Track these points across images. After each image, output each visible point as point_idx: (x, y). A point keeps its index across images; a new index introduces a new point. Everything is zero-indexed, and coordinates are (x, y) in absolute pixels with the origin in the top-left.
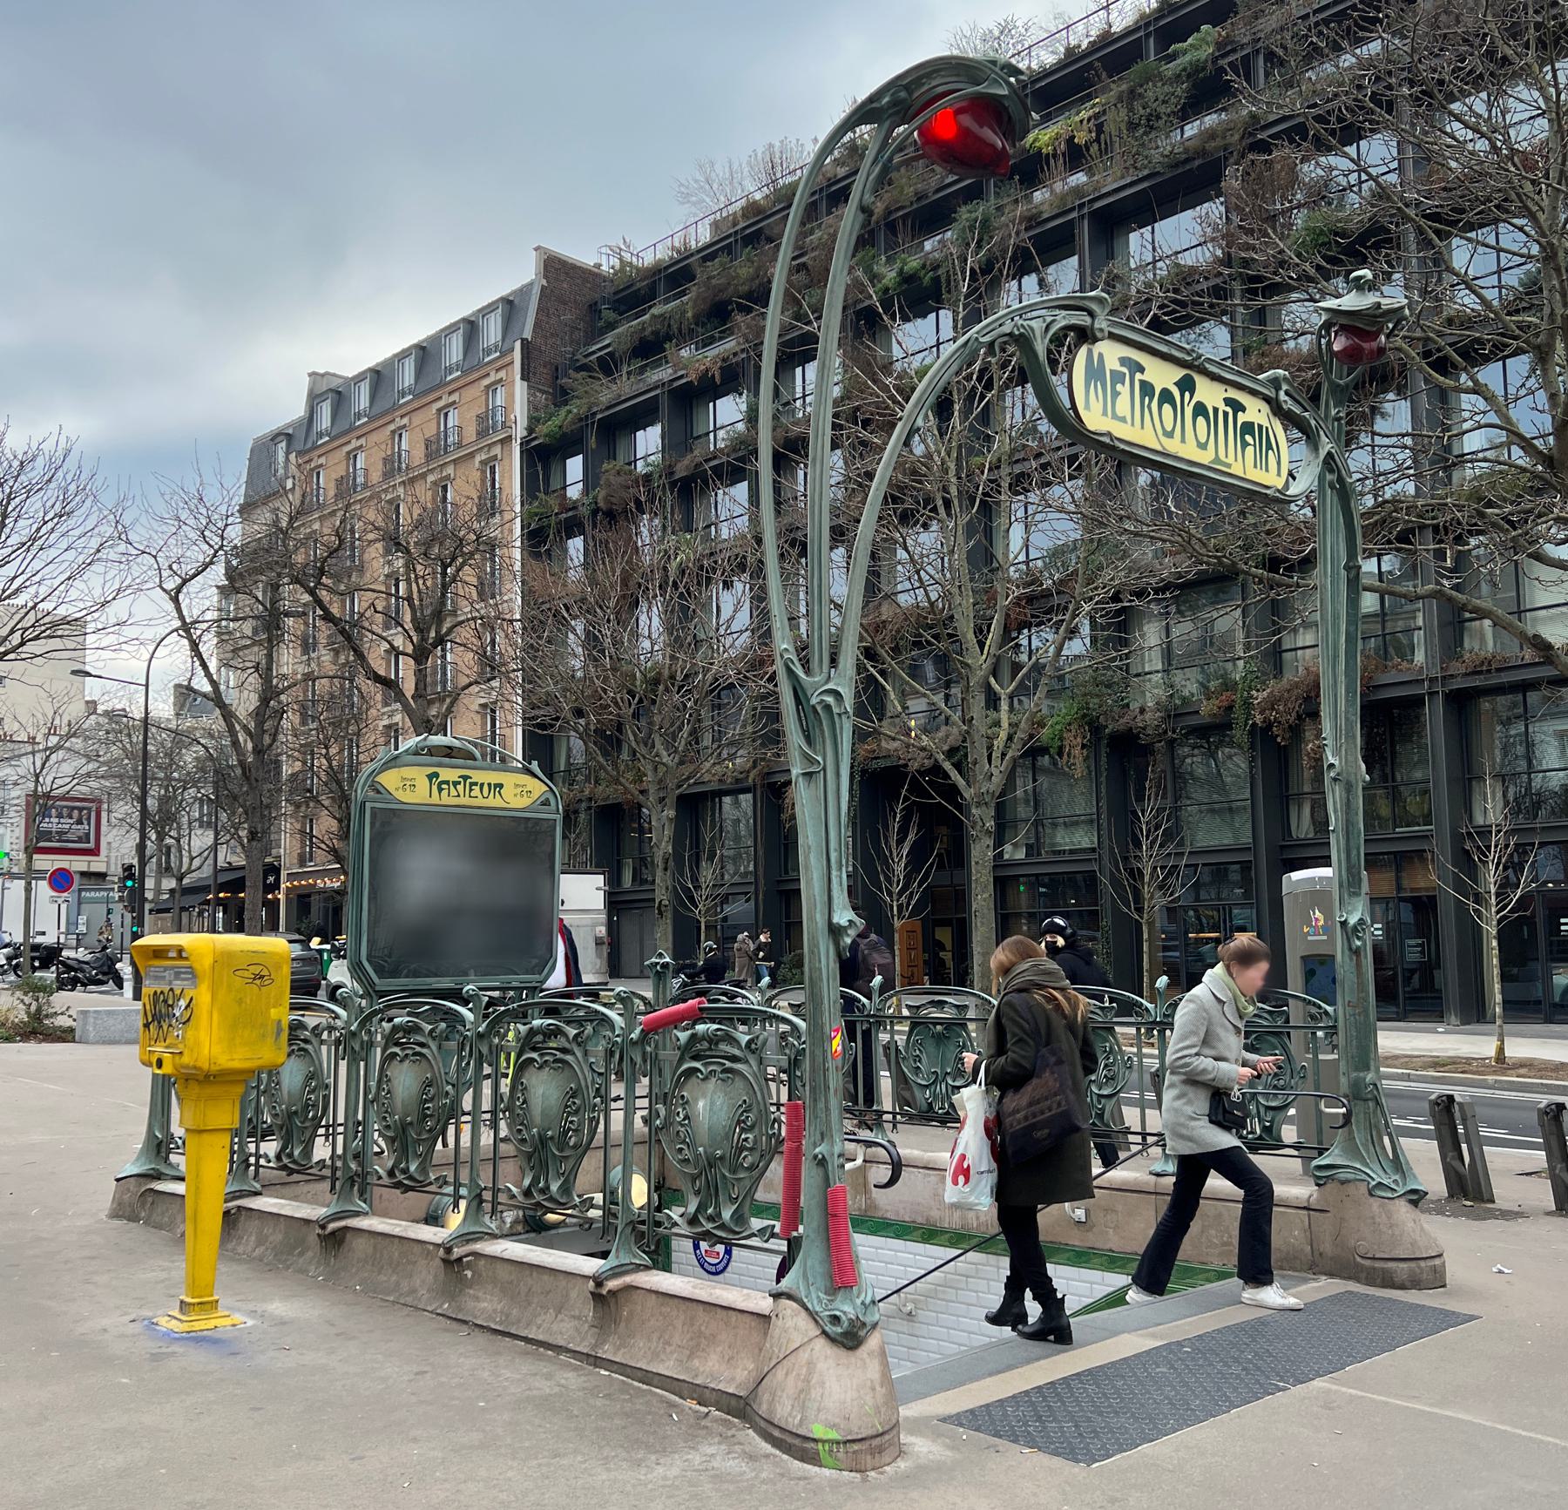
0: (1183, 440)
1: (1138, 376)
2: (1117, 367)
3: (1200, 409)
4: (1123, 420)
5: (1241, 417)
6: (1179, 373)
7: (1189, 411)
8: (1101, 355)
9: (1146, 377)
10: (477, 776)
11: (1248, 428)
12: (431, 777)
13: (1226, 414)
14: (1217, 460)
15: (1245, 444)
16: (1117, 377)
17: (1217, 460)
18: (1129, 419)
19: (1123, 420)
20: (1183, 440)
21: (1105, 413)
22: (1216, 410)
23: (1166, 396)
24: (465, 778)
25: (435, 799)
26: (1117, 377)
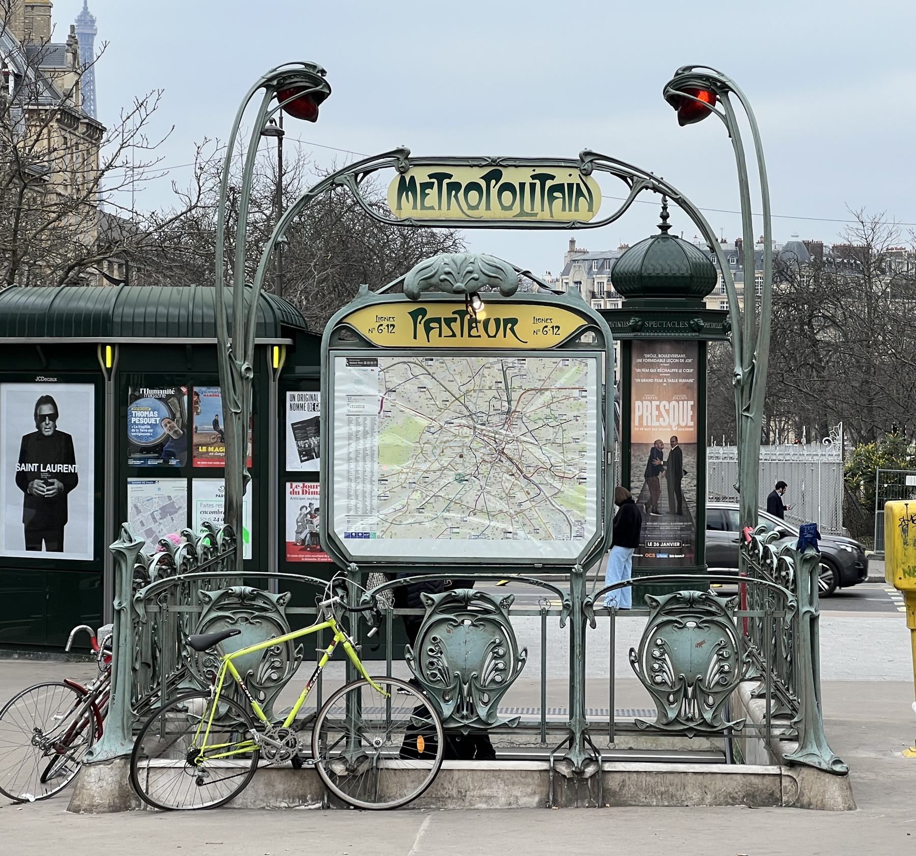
0: (488, 208)
1: (446, 181)
2: (428, 180)
3: (508, 187)
4: (432, 208)
5: (549, 183)
7: (494, 192)
8: (412, 178)
11: (559, 188)
13: (533, 186)
15: (552, 199)
16: (426, 186)
17: (522, 213)
18: (436, 207)
19: (432, 208)
20: (488, 208)
21: (415, 207)
22: (522, 185)
23: (473, 186)
26: (425, 186)
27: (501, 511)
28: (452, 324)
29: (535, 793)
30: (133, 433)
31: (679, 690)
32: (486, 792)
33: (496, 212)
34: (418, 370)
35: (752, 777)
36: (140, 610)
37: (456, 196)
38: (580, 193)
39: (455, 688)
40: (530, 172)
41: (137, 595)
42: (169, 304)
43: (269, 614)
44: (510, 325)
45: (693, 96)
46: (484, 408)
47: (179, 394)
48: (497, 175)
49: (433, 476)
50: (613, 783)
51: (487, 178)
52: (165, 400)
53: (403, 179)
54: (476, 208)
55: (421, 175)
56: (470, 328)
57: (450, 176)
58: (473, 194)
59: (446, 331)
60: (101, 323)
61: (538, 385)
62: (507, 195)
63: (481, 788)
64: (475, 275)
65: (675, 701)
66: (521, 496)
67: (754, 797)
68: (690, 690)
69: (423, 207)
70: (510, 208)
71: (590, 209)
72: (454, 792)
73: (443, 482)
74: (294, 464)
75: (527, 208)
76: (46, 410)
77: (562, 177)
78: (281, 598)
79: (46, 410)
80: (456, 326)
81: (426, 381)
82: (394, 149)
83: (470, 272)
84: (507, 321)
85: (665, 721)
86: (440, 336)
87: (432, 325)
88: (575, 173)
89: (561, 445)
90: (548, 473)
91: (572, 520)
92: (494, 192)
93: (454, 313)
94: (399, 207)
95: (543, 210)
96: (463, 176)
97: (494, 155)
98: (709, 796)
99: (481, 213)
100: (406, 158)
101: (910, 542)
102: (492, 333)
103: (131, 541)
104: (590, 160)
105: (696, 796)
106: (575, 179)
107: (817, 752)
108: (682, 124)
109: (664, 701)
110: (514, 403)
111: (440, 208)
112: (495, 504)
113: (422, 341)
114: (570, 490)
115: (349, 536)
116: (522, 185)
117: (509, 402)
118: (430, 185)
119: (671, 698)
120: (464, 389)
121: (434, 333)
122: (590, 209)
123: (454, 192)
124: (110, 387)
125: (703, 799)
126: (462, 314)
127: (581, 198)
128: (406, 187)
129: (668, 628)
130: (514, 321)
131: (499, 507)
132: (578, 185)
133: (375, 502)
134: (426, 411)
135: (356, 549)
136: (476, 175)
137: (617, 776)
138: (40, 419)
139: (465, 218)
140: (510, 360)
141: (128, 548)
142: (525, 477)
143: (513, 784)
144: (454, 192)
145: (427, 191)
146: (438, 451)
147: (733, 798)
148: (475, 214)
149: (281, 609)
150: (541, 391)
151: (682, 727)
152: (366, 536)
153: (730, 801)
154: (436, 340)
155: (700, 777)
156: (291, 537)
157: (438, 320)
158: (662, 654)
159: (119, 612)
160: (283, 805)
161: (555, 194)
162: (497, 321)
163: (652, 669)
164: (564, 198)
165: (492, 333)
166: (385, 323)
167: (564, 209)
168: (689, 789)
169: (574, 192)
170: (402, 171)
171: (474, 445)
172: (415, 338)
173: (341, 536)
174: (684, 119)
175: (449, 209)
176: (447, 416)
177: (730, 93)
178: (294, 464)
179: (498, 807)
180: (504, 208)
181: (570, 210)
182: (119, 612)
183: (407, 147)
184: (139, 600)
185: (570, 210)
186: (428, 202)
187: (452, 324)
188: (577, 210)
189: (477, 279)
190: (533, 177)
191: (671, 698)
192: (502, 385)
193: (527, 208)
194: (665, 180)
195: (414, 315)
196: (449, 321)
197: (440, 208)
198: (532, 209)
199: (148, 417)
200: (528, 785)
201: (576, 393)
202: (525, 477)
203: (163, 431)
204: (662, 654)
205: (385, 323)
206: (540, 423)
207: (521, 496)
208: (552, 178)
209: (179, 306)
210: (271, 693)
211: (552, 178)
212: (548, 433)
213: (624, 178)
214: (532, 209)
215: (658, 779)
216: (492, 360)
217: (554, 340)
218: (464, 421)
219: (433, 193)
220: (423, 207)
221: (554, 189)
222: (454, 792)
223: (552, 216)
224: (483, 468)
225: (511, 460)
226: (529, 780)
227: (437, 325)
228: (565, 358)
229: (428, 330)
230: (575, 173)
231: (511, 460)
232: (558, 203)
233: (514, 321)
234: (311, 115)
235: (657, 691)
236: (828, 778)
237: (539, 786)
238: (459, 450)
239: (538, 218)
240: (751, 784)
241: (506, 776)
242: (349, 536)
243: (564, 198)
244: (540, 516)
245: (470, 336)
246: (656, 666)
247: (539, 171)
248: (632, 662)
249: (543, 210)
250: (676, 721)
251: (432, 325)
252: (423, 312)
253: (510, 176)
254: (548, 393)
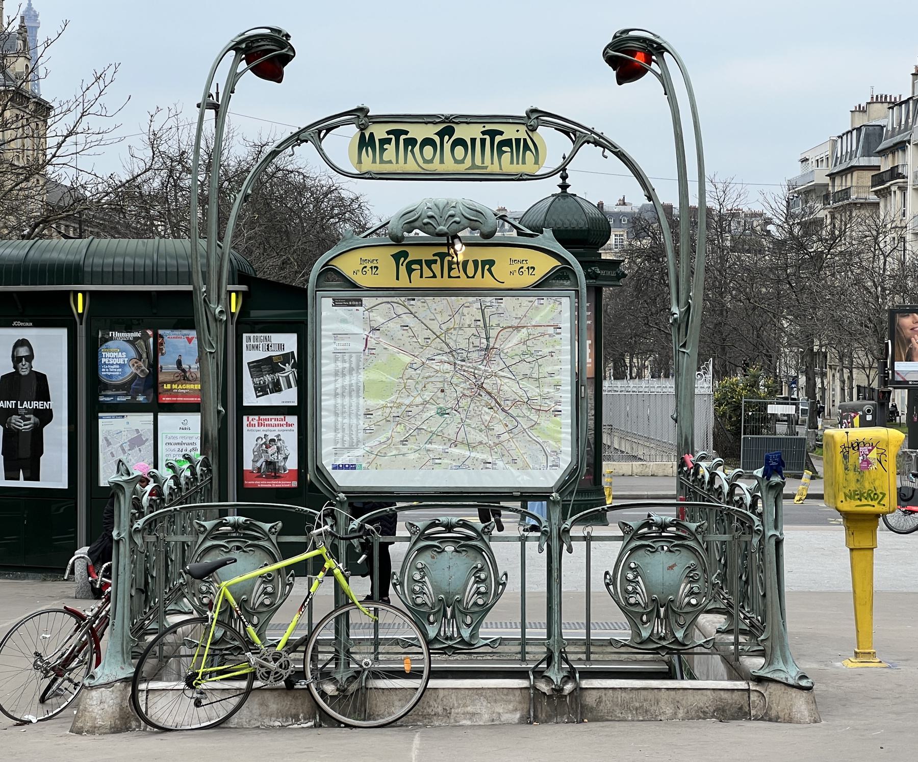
0: (442, 161)
1: (403, 137)
2: (386, 136)
3: (460, 142)
4: (390, 162)
5: (498, 138)
7: (447, 147)
8: (372, 134)
9: (409, 136)
11: (508, 143)
13: (483, 141)
14: (474, 166)
15: (501, 153)
17: (474, 166)
18: (394, 161)
19: (390, 162)
20: (442, 161)
21: (374, 161)
22: (473, 140)
23: (428, 142)
26: (383, 142)
27: (481, 443)
28: (433, 266)
29: (516, 710)
30: (103, 372)
31: (652, 611)
32: (470, 709)
33: (449, 165)
34: (400, 310)
35: (722, 693)
36: (138, 540)
37: (412, 151)
38: (526, 147)
39: (439, 610)
40: (480, 128)
41: (136, 526)
42: (135, 255)
43: (261, 543)
44: (487, 267)
45: (631, 57)
46: (464, 344)
47: (145, 338)
48: (449, 131)
49: (415, 410)
50: (590, 699)
51: (441, 134)
52: (132, 342)
53: (362, 136)
54: (431, 161)
55: (380, 131)
56: (450, 269)
57: (406, 133)
58: (428, 149)
59: (427, 272)
60: (73, 272)
61: (515, 323)
62: (459, 150)
63: (465, 706)
64: (457, 219)
65: (648, 621)
66: (499, 428)
67: (724, 711)
68: (662, 610)
69: (382, 161)
70: (462, 161)
71: (536, 162)
72: (440, 710)
73: (425, 415)
74: (250, 399)
75: (478, 161)
76: (23, 351)
77: (510, 132)
78: (273, 527)
79: (23, 351)
80: (436, 268)
81: (408, 319)
82: (355, 107)
83: (452, 216)
84: (484, 263)
85: (638, 640)
86: (421, 277)
87: (413, 267)
88: (523, 129)
89: (537, 380)
90: (525, 406)
91: (548, 450)
92: (447, 147)
93: (434, 255)
94: (360, 162)
95: (492, 163)
96: (418, 132)
97: (447, 112)
98: (681, 711)
99: (436, 166)
100: (366, 116)
101: (851, 467)
102: (471, 274)
103: (129, 474)
104: (535, 118)
105: (669, 711)
106: (522, 135)
107: (784, 668)
108: (620, 83)
109: (638, 621)
110: (492, 340)
111: (397, 162)
112: (475, 436)
113: (404, 282)
114: (546, 422)
115: (336, 467)
116: (473, 140)
117: (488, 339)
118: (388, 141)
119: (644, 618)
120: (444, 327)
121: (416, 275)
122: (536, 162)
123: (410, 147)
124: (82, 330)
125: (675, 714)
126: (442, 256)
127: (528, 152)
128: (366, 142)
129: (641, 552)
130: (492, 263)
131: (479, 439)
132: (525, 140)
133: (361, 435)
134: (408, 348)
135: (342, 479)
136: (430, 131)
137: (594, 692)
138: (16, 360)
139: (420, 171)
140: (488, 299)
141: (125, 481)
142: (503, 410)
143: (496, 701)
144: (410, 147)
145: (385, 146)
146: (420, 386)
147: (704, 712)
148: (430, 167)
149: (273, 538)
150: (518, 328)
151: (655, 646)
152: (352, 467)
153: (702, 715)
154: (417, 281)
155: (673, 693)
156: (248, 465)
157: (419, 262)
158: (636, 577)
159: (118, 542)
160: (277, 724)
161: (504, 149)
162: (476, 262)
163: (626, 591)
164: (512, 152)
165: (471, 274)
166: (369, 265)
167: (512, 163)
168: (662, 704)
169: (522, 147)
170: (362, 128)
171: (455, 380)
172: (398, 279)
173: (329, 468)
174: (621, 80)
175: (405, 163)
176: (429, 352)
177: (666, 54)
178: (250, 399)
179: (481, 723)
180: (456, 161)
181: (518, 163)
182: (118, 542)
183: (366, 105)
184: (137, 531)
185: (518, 163)
186: (386, 156)
187: (433, 266)
188: (524, 163)
189: (458, 223)
190: (484, 133)
191: (644, 618)
192: (481, 323)
193: (478, 161)
194: (605, 135)
195: (396, 257)
196: (429, 263)
197: (397, 162)
198: (483, 163)
199: (118, 357)
200: (510, 702)
201: (551, 330)
202: (503, 410)
203: (131, 370)
204: (636, 577)
205: (369, 265)
206: (517, 359)
207: (499, 428)
208: (501, 133)
209: (145, 256)
210: (264, 618)
211: (501, 133)
212: (524, 368)
213: (567, 134)
214: (483, 163)
215: (633, 695)
216: (471, 299)
217: (529, 280)
218: (445, 358)
219: (391, 148)
220: (382, 161)
222: (440, 710)
223: (501, 169)
224: (464, 402)
225: (489, 394)
226: (511, 697)
227: (418, 267)
228: (540, 297)
229: (410, 271)
230: (523, 129)
231: (489, 394)
232: (506, 157)
233: (492, 263)
234: (277, 77)
235: (631, 612)
236: (794, 693)
237: (520, 703)
238: (440, 385)
239: (488, 171)
240: (721, 699)
241: (489, 693)
242: (336, 467)
243: (512, 152)
244: (518, 447)
245: (450, 277)
246: (630, 588)
247: (489, 127)
248: (607, 585)
249: (492, 163)
250: (649, 640)
251: (413, 267)
252: (405, 254)
253: (462, 132)
254: (524, 330)
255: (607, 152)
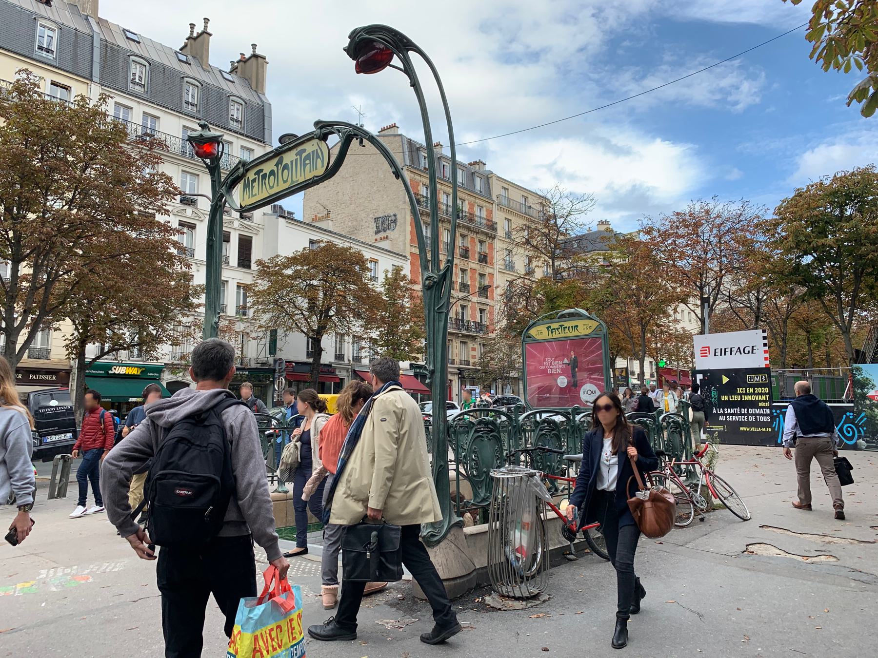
5: (304, 155)
6: (276, 160)
10: (566, 324)
12: (548, 328)
15: (305, 165)
17: (292, 181)
22: (292, 162)
23: (272, 173)
24: (561, 326)
25: (551, 337)
38: (318, 157)
51: (277, 165)
57: (262, 170)
69: (253, 196)
70: (286, 181)
75: (294, 179)
208: (304, 150)
219: (256, 184)
221: (308, 157)
230: (315, 141)
255: (365, 142)
